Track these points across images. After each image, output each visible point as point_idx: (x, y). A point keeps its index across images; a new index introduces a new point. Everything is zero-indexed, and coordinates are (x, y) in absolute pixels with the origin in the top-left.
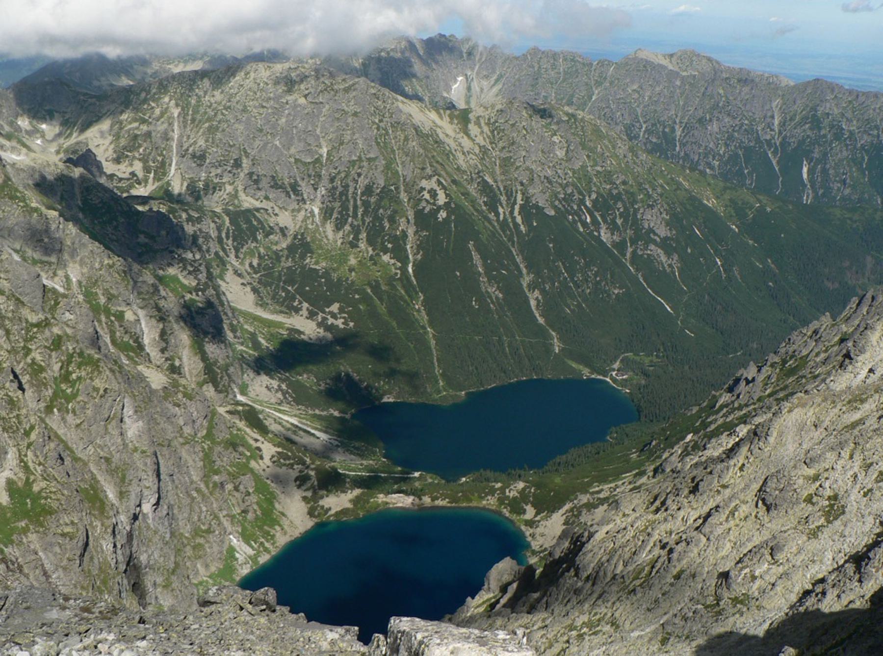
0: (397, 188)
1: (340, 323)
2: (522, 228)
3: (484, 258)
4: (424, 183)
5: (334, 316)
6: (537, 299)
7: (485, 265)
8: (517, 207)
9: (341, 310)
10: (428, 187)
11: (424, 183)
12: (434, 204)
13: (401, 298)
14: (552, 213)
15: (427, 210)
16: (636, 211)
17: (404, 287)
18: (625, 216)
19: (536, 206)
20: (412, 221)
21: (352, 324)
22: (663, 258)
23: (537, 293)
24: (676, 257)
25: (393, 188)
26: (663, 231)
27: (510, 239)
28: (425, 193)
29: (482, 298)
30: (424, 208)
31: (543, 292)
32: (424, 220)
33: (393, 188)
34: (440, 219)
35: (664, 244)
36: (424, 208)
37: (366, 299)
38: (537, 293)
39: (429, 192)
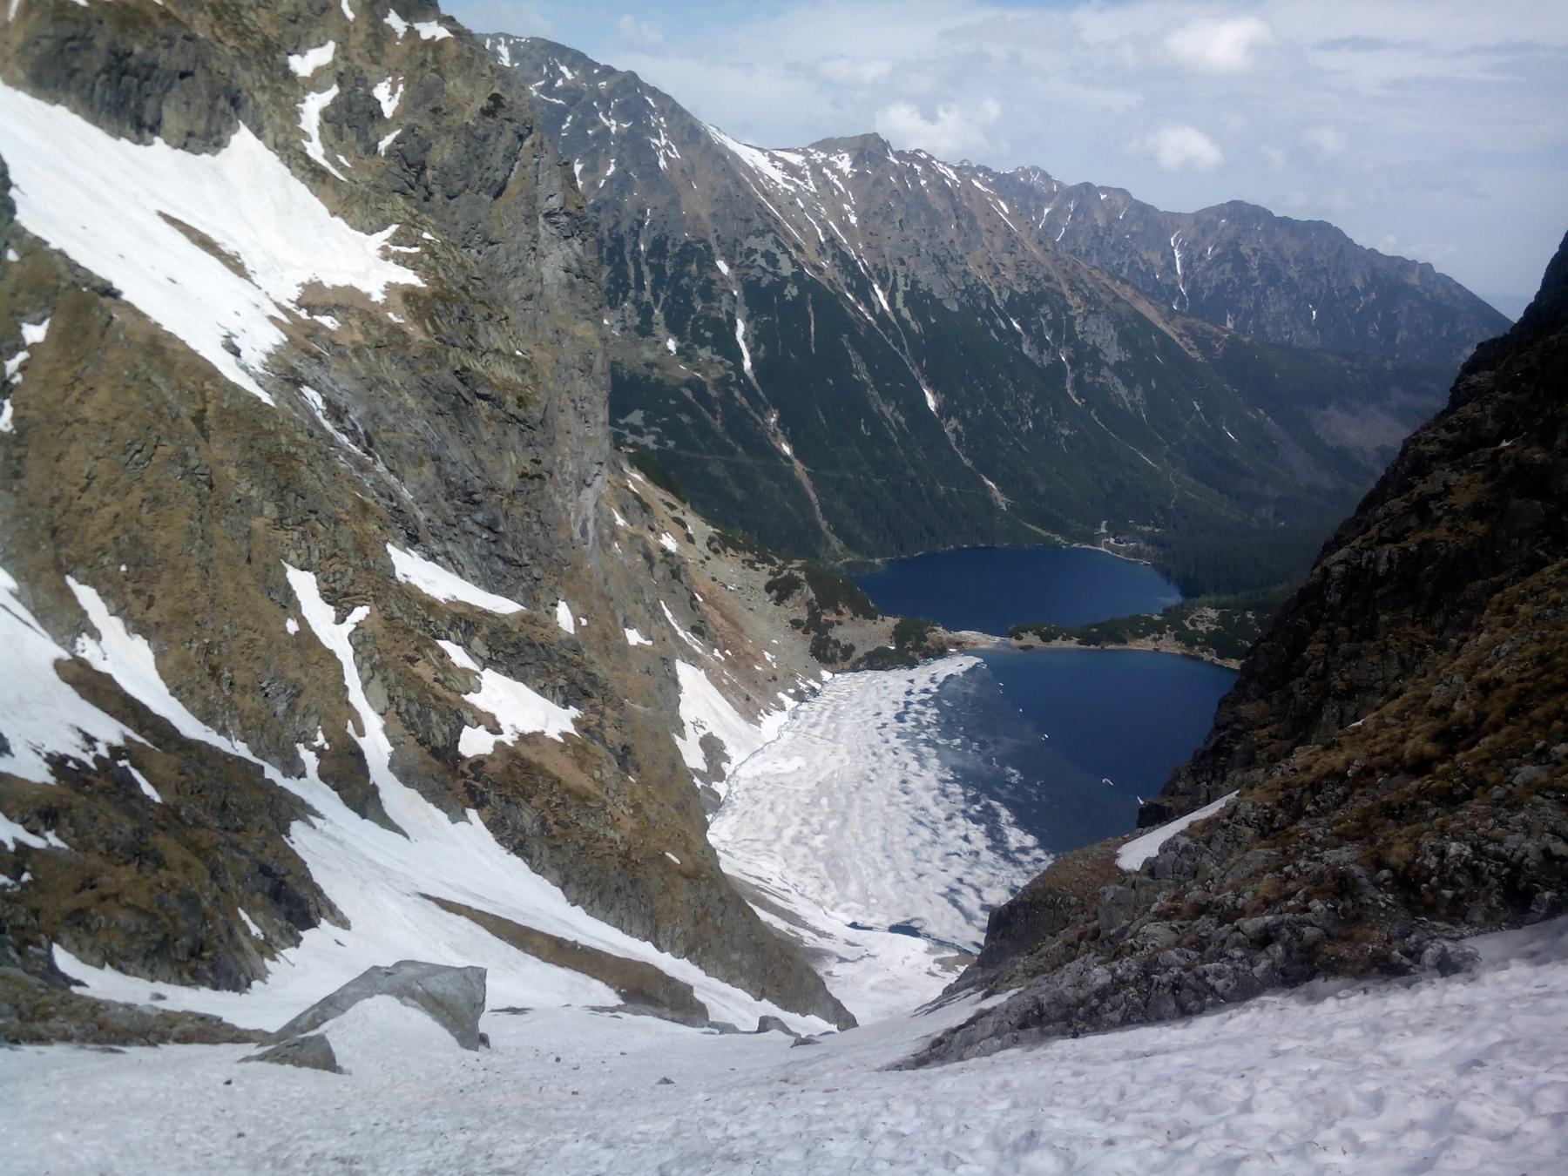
0: (708, 248)
1: (649, 441)
2: (913, 324)
3: (868, 359)
4: (753, 242)
5: (636, 430)
6: (955, 431)
7: (870, 370)
8: (899, 296)
9: (648, 421)
10: (761, 249)
11: (753, 242)
12: (775, 274)
13: (743, 411)
14: (956, 308)
15: (764, 282)
16: (1071, 320)
17: (743, 394)
18: (1055, 325)
19: (929, 294)
20: (741, 299)
21: (671, 443)
22: (1123, 391)
23: (954, 422)
24: (1139, 391)
25: (701, 246)
26: (1113, 354)
27: (897, 342)
28: (758, 256)
29: (875, 420)
30: (759, 279)
31: (963, 420)
32: (759, 298)
33: (701, 246)
34: (789, 298)
35: (1119, 368)
36: (759, 279)
37: (685, 406)
38: (954, 422)
39: (763, 256)
